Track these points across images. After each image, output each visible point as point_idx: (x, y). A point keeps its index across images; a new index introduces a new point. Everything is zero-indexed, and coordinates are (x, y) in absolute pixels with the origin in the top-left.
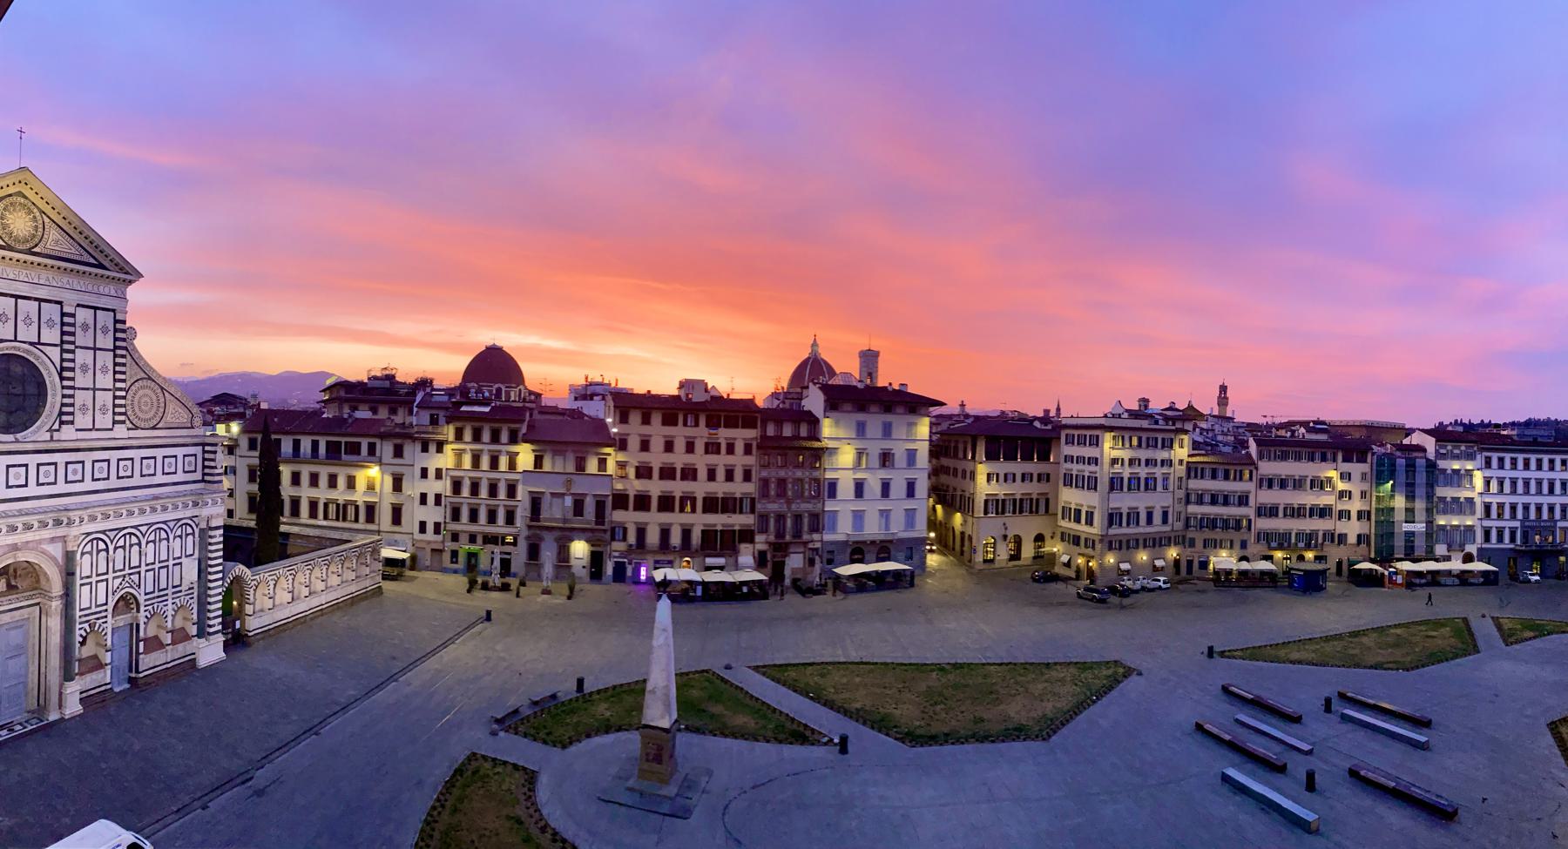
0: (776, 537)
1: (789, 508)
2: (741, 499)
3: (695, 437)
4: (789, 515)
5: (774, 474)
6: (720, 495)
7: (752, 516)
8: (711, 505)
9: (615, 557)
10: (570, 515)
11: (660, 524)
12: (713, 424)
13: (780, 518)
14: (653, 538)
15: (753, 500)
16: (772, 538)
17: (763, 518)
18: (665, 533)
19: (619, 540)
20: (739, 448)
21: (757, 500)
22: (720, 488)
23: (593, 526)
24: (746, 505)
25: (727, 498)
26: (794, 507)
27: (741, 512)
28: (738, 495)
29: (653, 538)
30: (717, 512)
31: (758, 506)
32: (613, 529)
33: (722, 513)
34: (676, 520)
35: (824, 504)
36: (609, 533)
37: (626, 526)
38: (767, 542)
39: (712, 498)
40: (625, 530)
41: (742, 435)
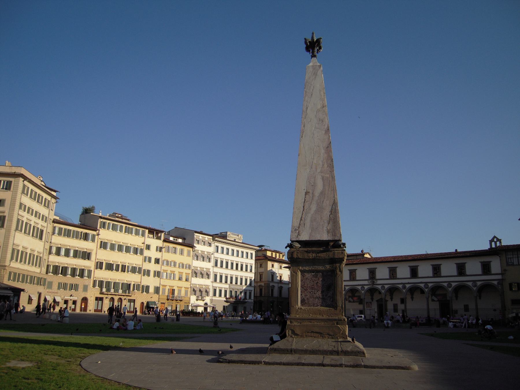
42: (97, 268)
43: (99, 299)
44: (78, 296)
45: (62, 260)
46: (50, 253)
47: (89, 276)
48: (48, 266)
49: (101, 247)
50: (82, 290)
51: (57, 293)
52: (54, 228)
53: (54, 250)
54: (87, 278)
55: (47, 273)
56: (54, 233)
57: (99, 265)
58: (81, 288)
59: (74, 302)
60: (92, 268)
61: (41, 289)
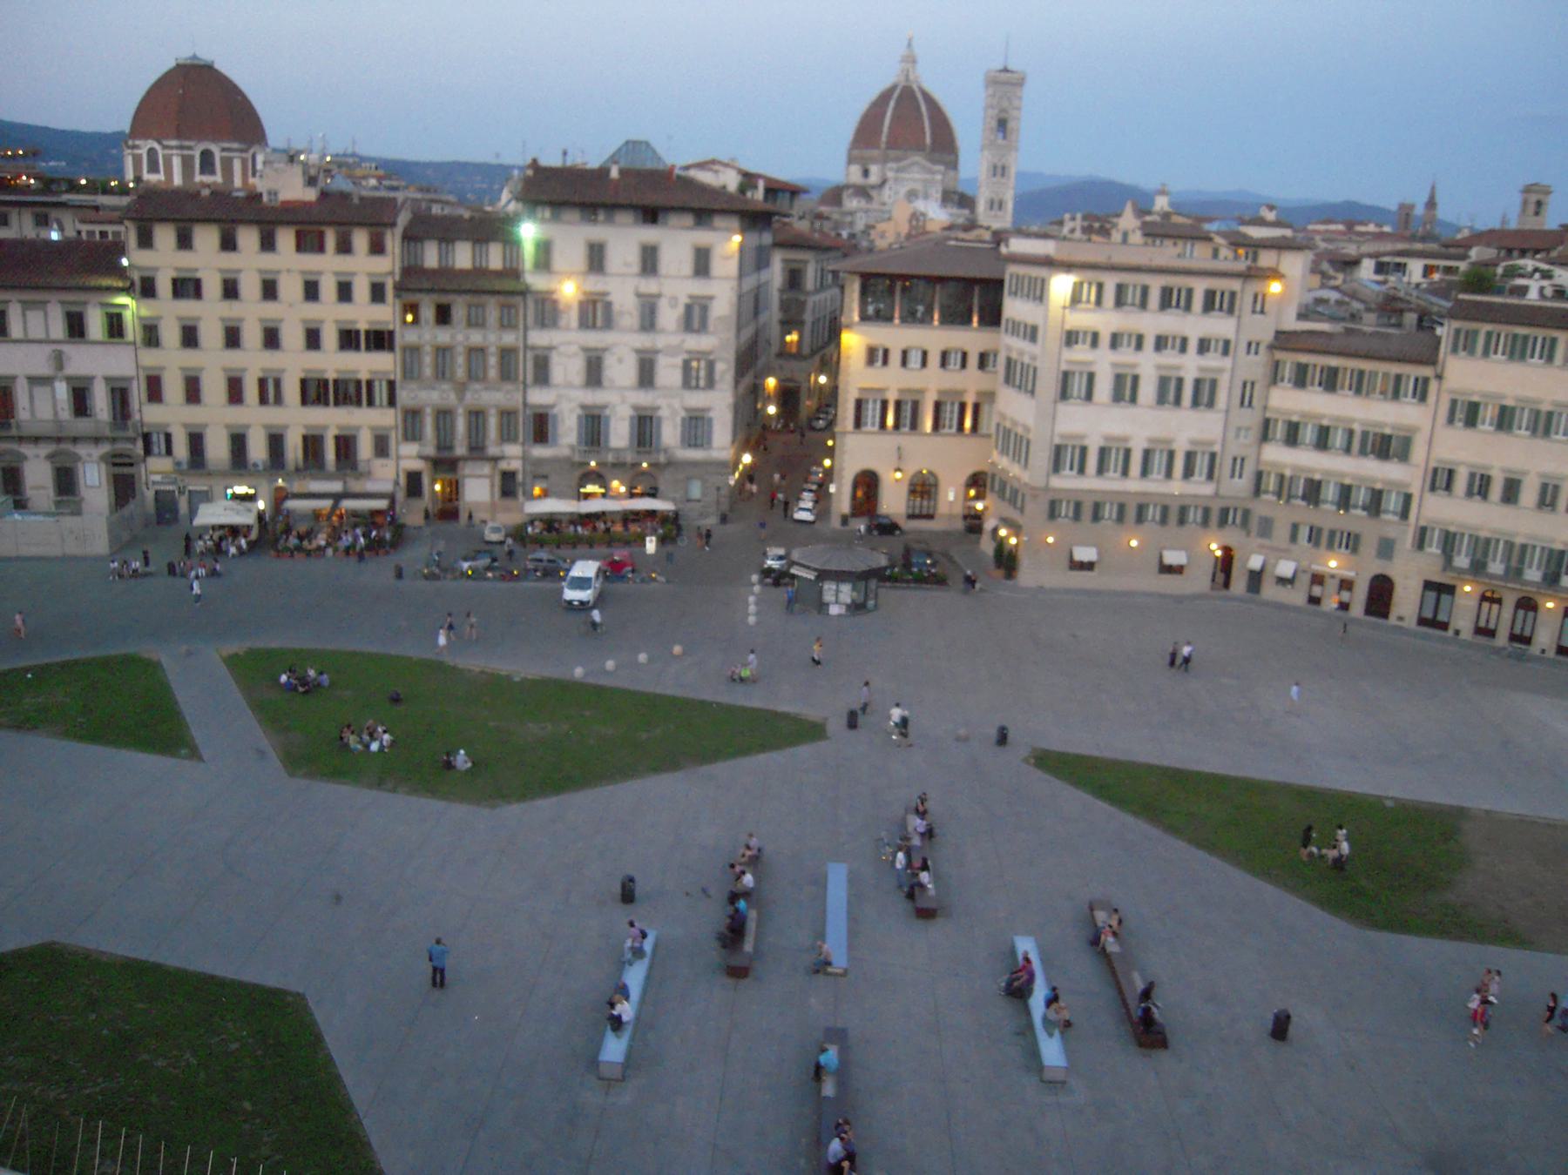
0: (439, 448)
1: (461, 398)
2: (370, 384)
3: (278, 272)
4: (460, 411)
5: (429, 335)
6: (331, 376)
7: (391, 412)
8: (316, 391)
9: (154, 483)
10: (66, 413)
11: (227, 426)
12: (309, 242)
13: (444, 416)
14: (217, 449)
15: (391, 385)
16: (430, 450)
17: (412, 416)
18: (238, 442)
19: (160, 454)
20: (361, 290)
21: (398, 385)
22: (333, 362)
23: (108, 432)
24: (381, 393)
25: (346, 382)
26: (468, 396)
27: (371, 403)
28: (364, 376)
29: (217, 449)
30: (326, 404)
31: (405, 396)
32: (147, 438)
33: (337, 403)
34: (255, 418)
35: (525, 393)
36: (140, 444)
37: (170, 430)
38: (421, 457)
39: (319, 380)
40: (168, 438)
41: (363, 265)
42: (1433, 488)
43: (1440, 590)
44: (1363, 568)
45: (1305, 460)
46: (1265, 435)
47: (1404, 514)
48: (1259, 476)
49: (1451, 420)
50: (1374, 552)
51: (1286, 551)
52: (1276, 366)
53: (1280, 431)
54: (1396, 518)
55: (1257, 490)
56: (1275, 378)
57: (1441, 479)
58: (1369, 547)
59: (1346, 585)
60: (1415, 490)
61: (1233, 537)
